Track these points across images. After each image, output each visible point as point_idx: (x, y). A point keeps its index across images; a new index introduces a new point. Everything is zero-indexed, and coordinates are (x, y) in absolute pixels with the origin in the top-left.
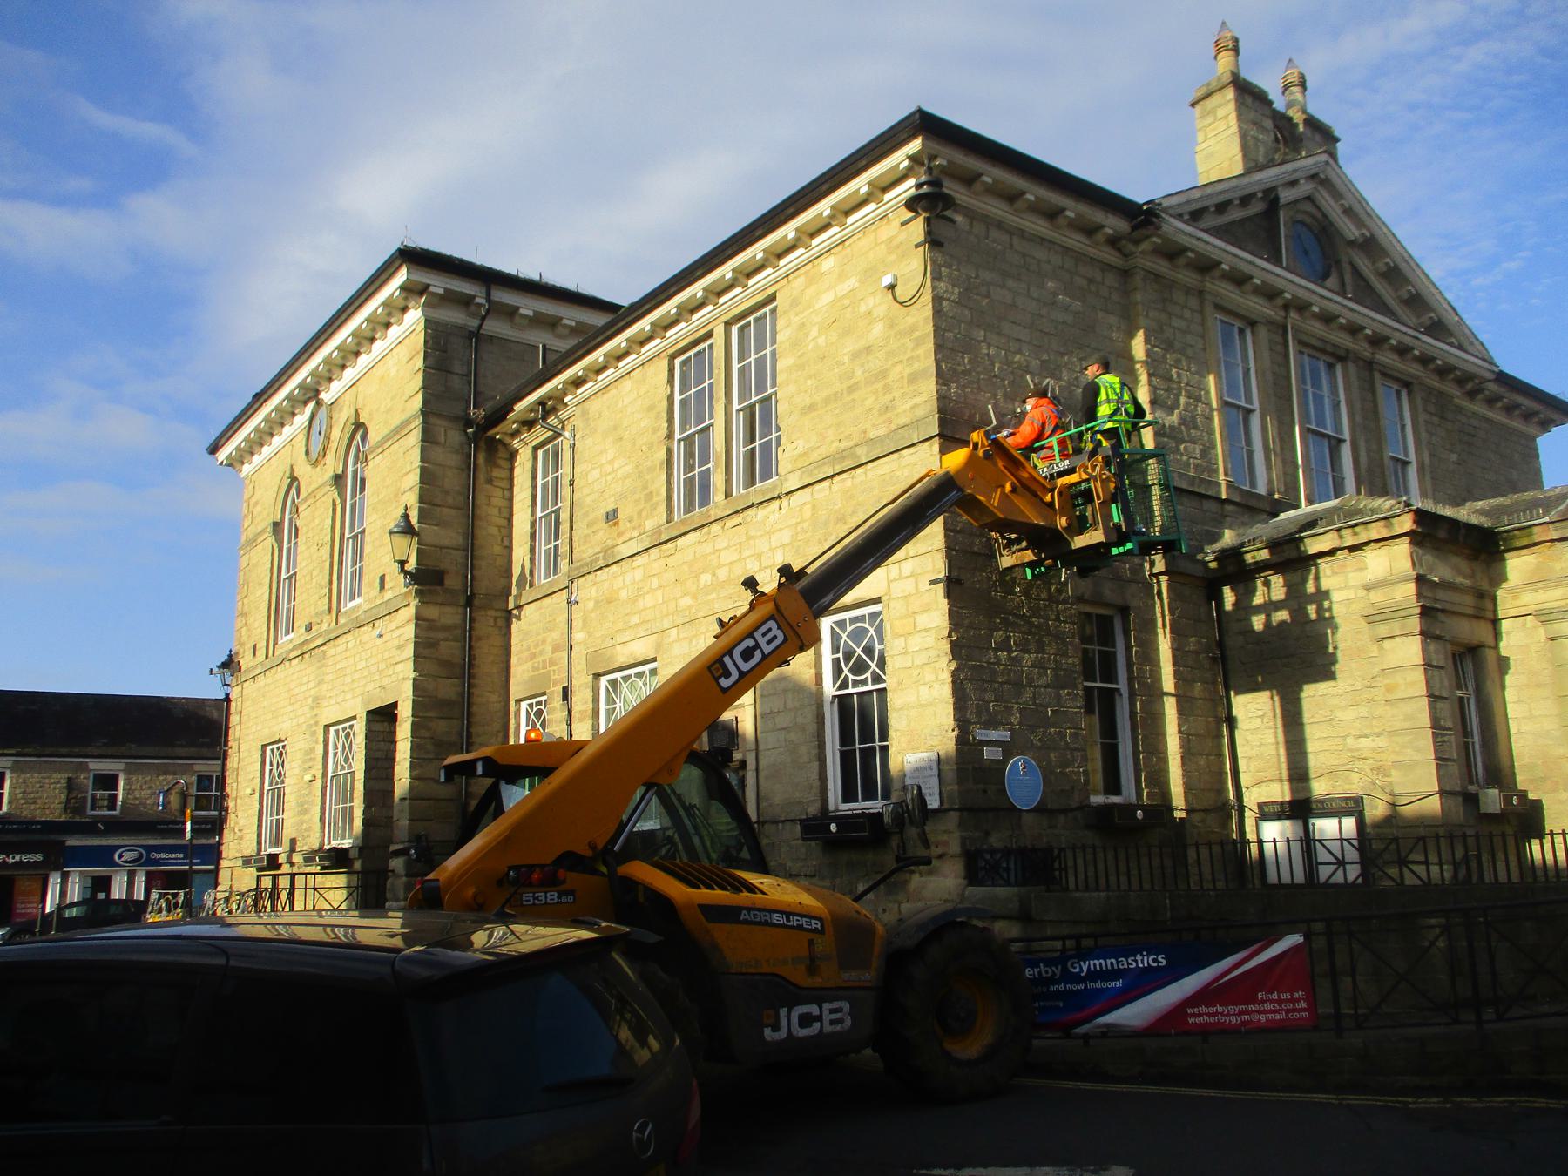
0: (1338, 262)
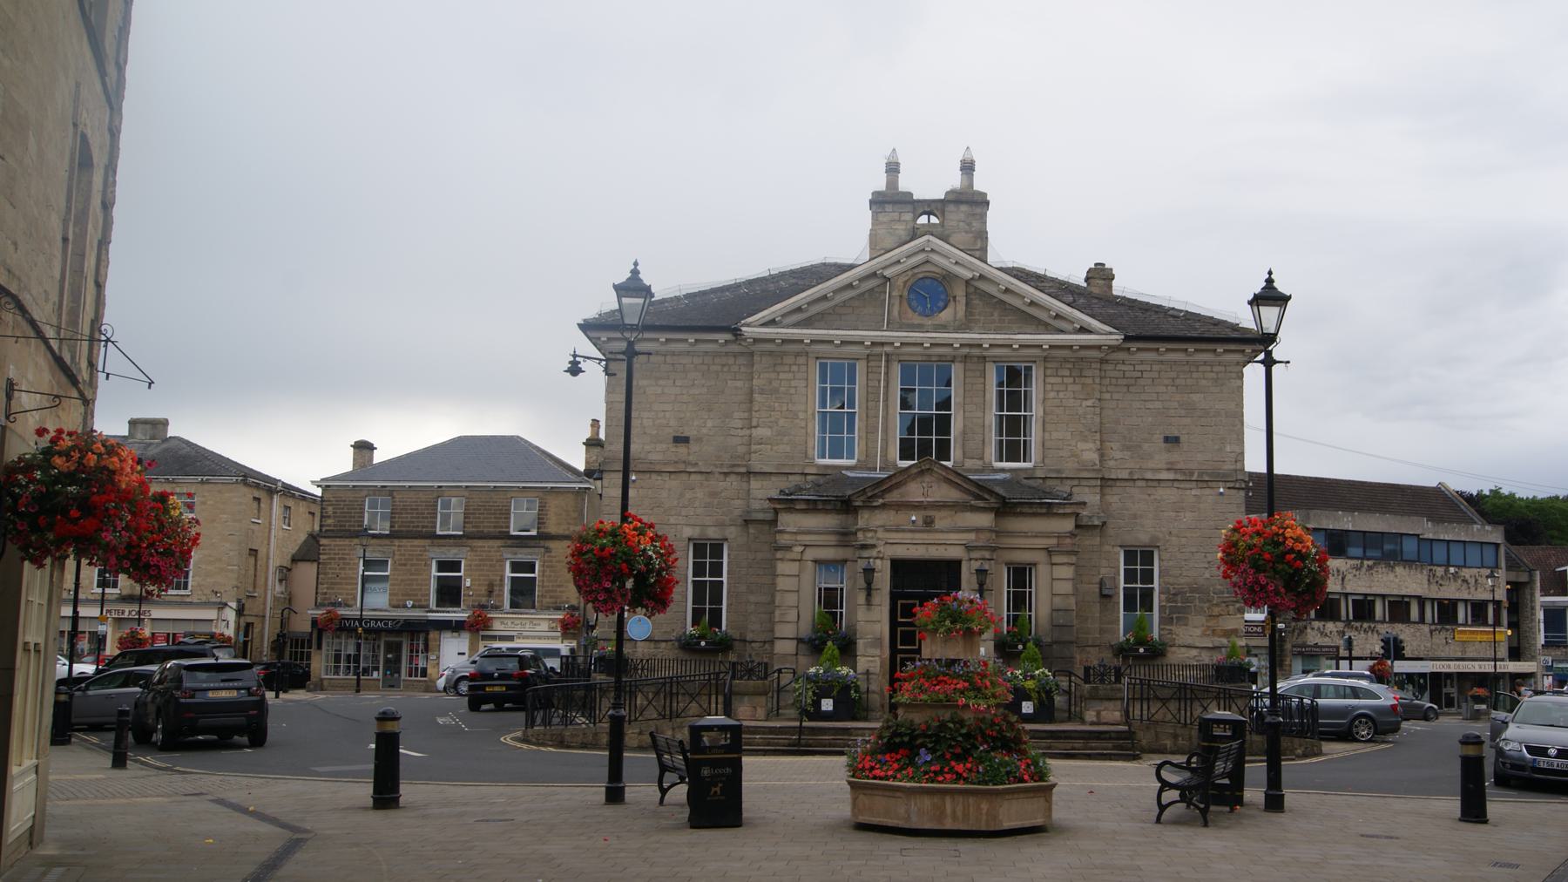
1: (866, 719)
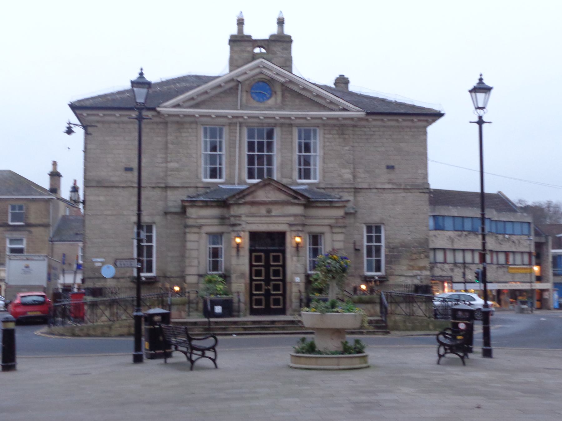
0: (275, 93)
1: (238, 316)
